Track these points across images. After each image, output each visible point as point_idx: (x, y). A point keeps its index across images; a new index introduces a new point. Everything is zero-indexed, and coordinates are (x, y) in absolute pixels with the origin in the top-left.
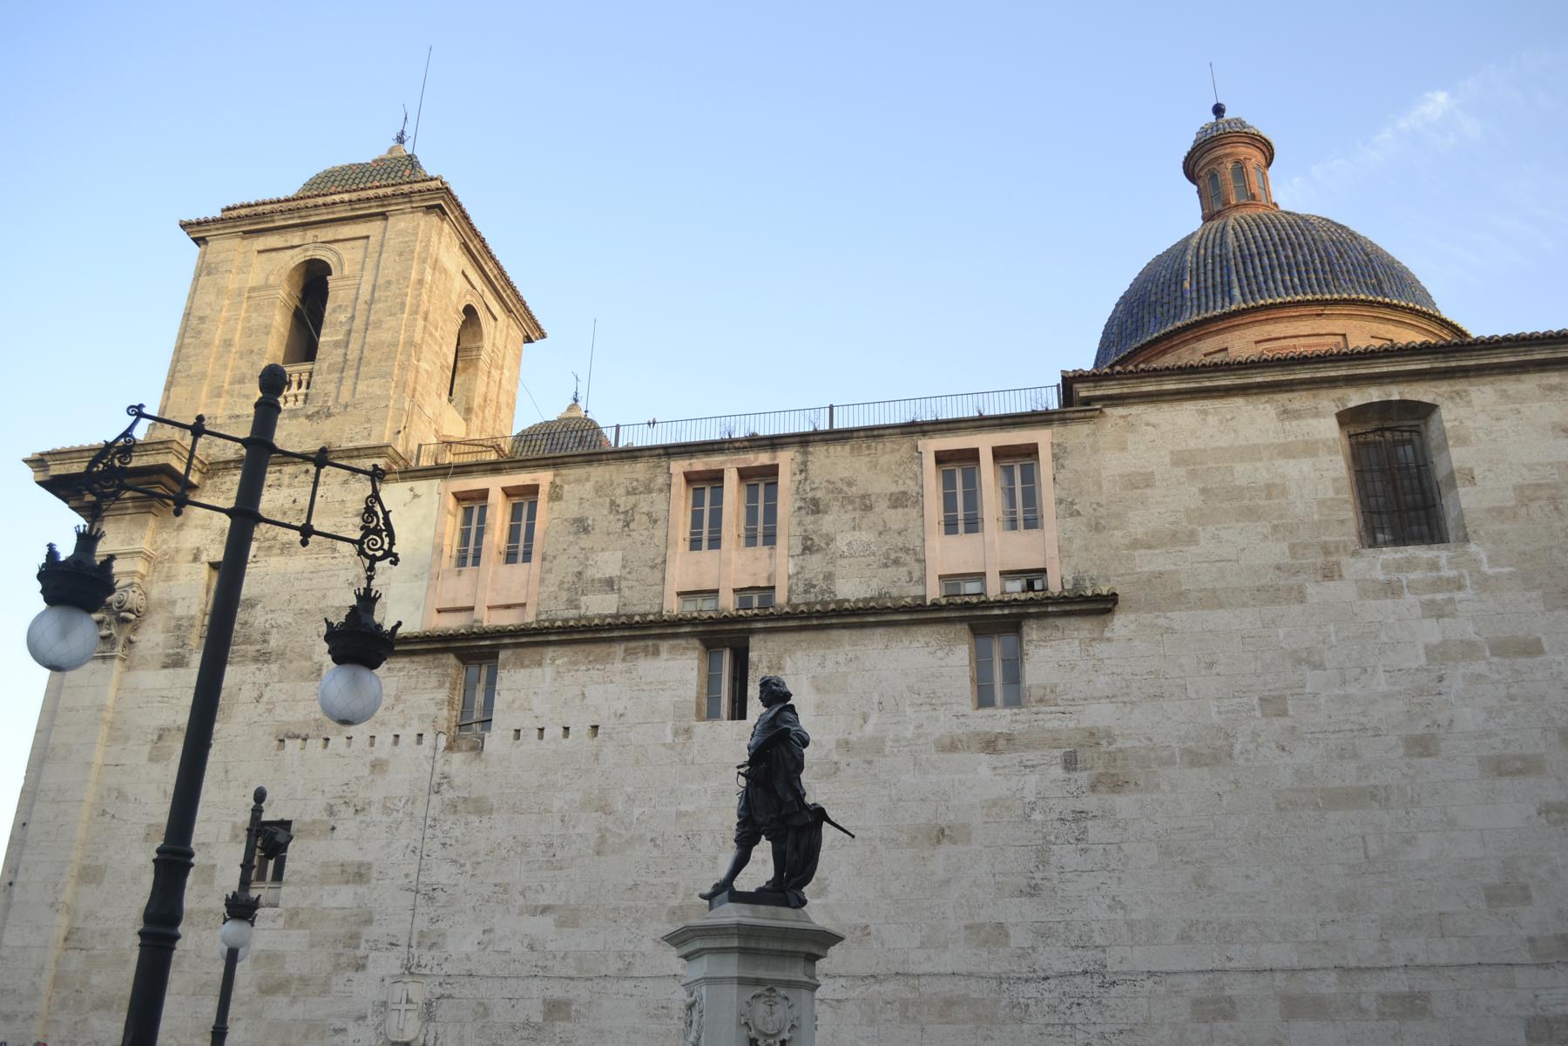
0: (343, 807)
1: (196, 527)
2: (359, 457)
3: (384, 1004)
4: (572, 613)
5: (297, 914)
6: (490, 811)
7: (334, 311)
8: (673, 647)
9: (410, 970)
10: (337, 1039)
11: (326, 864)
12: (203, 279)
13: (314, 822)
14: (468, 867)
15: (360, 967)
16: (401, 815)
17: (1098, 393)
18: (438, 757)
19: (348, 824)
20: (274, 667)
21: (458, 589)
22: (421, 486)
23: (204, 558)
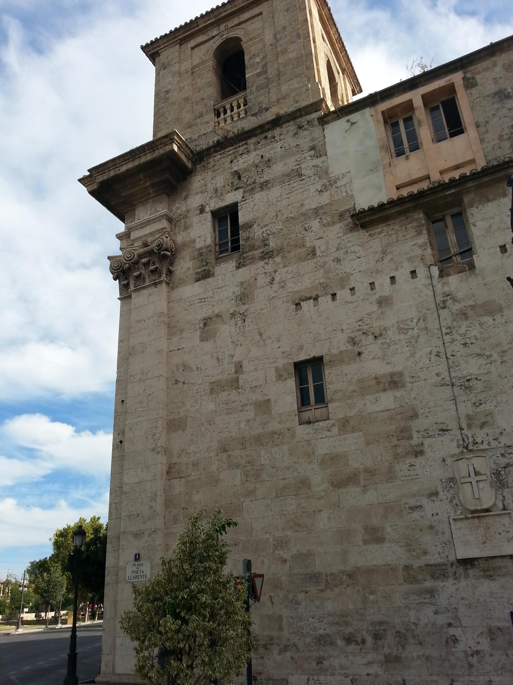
0: (363, 337)
1: (197, 194)
2: (301, 116)
3: (452, 480)
5: (348, 421)
6: (501, 310)
7: (251, 58)
9: (468, 448)
10: (416, 515)
11: (361, 381)
12: (162, 73)
13: (341, 352)
14: (495, 356)
15: (419, 453)
16: (416, 331)
18: (435, 283)
19: (371, 348)
20: (278, 259)
21: (410, 168)
22: (355, 117)
23: (207, 209)
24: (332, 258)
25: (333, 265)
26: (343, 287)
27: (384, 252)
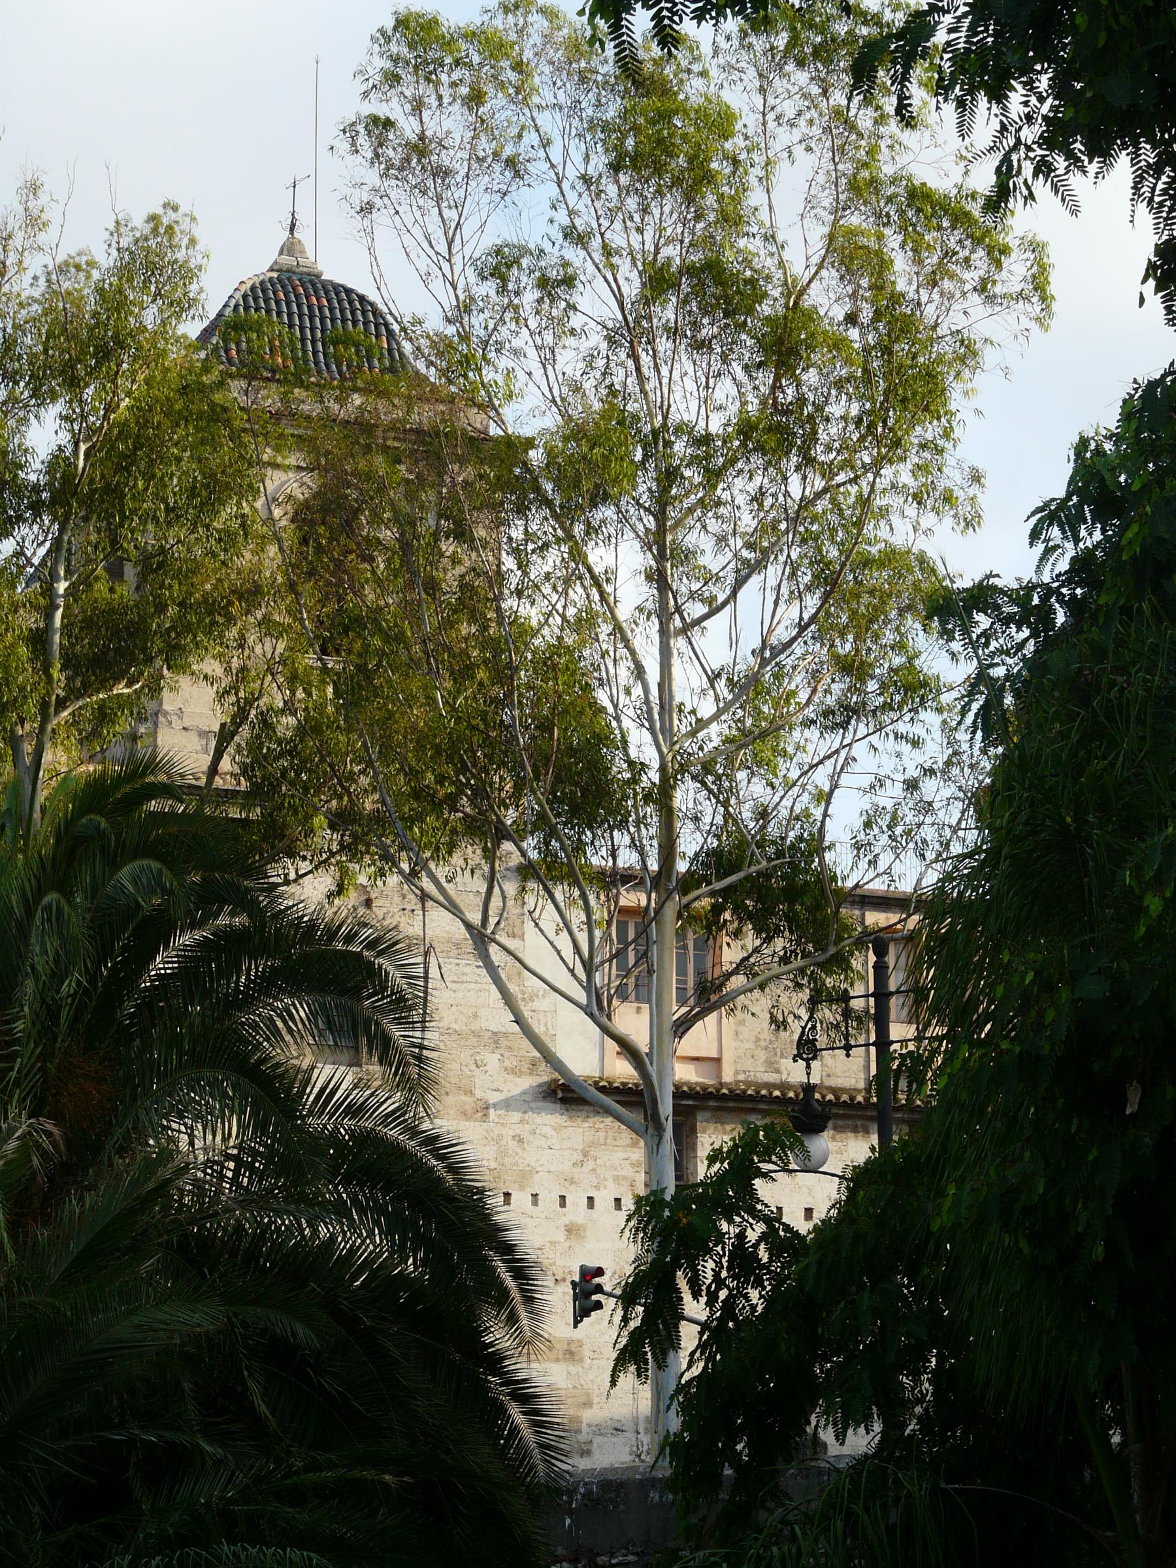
4: (772, 1078)
24: (512, 1133)
25: (513, 1144)
26: (522, 1188)
27: (585, 1154)
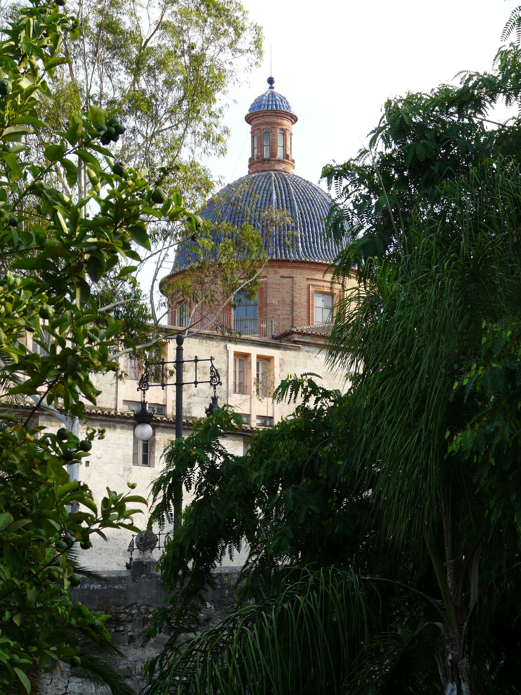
8: (122, 428)
17: (302, 340)
